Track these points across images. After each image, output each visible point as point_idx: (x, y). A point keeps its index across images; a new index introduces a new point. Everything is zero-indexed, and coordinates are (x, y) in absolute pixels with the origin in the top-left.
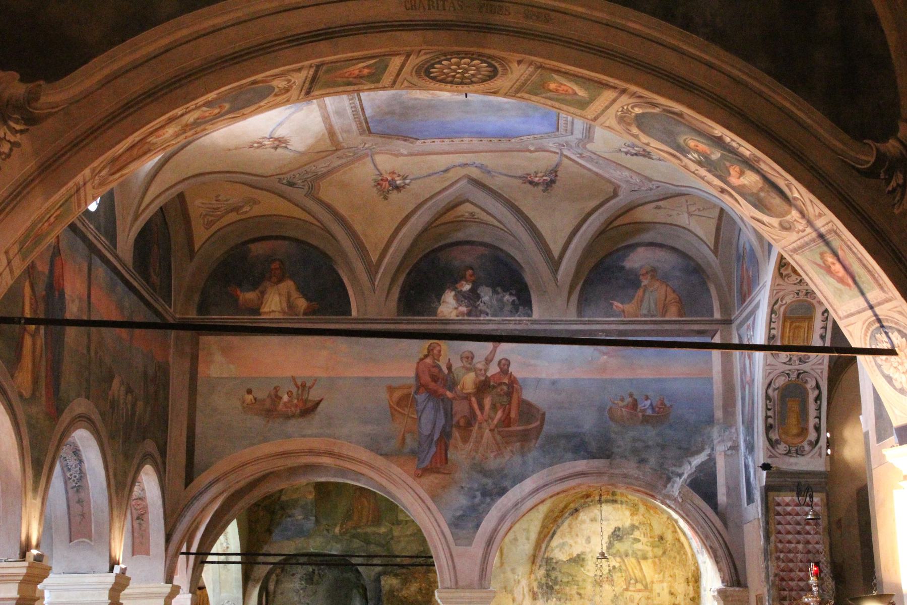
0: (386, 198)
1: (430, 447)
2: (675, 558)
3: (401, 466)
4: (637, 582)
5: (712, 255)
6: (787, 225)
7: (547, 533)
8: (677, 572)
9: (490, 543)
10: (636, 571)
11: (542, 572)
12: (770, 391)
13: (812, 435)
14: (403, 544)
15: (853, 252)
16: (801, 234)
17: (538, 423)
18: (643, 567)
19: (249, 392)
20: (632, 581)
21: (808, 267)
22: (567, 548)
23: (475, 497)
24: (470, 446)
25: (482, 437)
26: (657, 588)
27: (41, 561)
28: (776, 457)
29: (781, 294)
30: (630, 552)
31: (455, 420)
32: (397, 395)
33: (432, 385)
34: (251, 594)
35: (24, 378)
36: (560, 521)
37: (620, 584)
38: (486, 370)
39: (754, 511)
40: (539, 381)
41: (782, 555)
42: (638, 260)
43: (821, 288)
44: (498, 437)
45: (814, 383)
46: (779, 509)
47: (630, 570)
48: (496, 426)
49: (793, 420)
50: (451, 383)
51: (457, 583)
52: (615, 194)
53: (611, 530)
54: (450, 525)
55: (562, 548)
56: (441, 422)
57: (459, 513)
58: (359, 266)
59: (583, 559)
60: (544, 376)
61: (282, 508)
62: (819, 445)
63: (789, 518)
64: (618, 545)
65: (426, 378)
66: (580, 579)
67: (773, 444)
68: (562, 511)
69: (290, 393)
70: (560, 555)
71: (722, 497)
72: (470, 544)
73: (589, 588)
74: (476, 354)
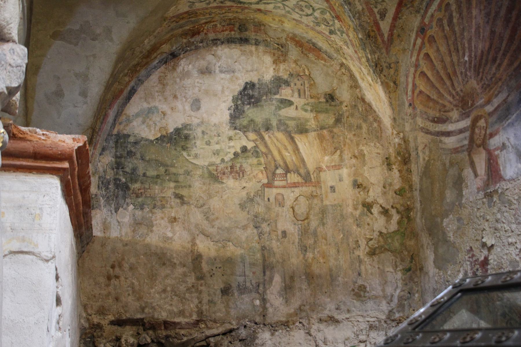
2: (359, 127)
4: (287, 170)
7: (120, 89)
8: (365, 149)
10: (286, 154)
20: (279, 171)
22: (156, 118)
26: (329, 178)
30: (274, 123)
36: (143, 72)
37: (256, 175)
47: (276, 153)
55: (150, 115)
59: (187, 137)
66: (181, 171)
68: (148, 55)
73: (197, 187)
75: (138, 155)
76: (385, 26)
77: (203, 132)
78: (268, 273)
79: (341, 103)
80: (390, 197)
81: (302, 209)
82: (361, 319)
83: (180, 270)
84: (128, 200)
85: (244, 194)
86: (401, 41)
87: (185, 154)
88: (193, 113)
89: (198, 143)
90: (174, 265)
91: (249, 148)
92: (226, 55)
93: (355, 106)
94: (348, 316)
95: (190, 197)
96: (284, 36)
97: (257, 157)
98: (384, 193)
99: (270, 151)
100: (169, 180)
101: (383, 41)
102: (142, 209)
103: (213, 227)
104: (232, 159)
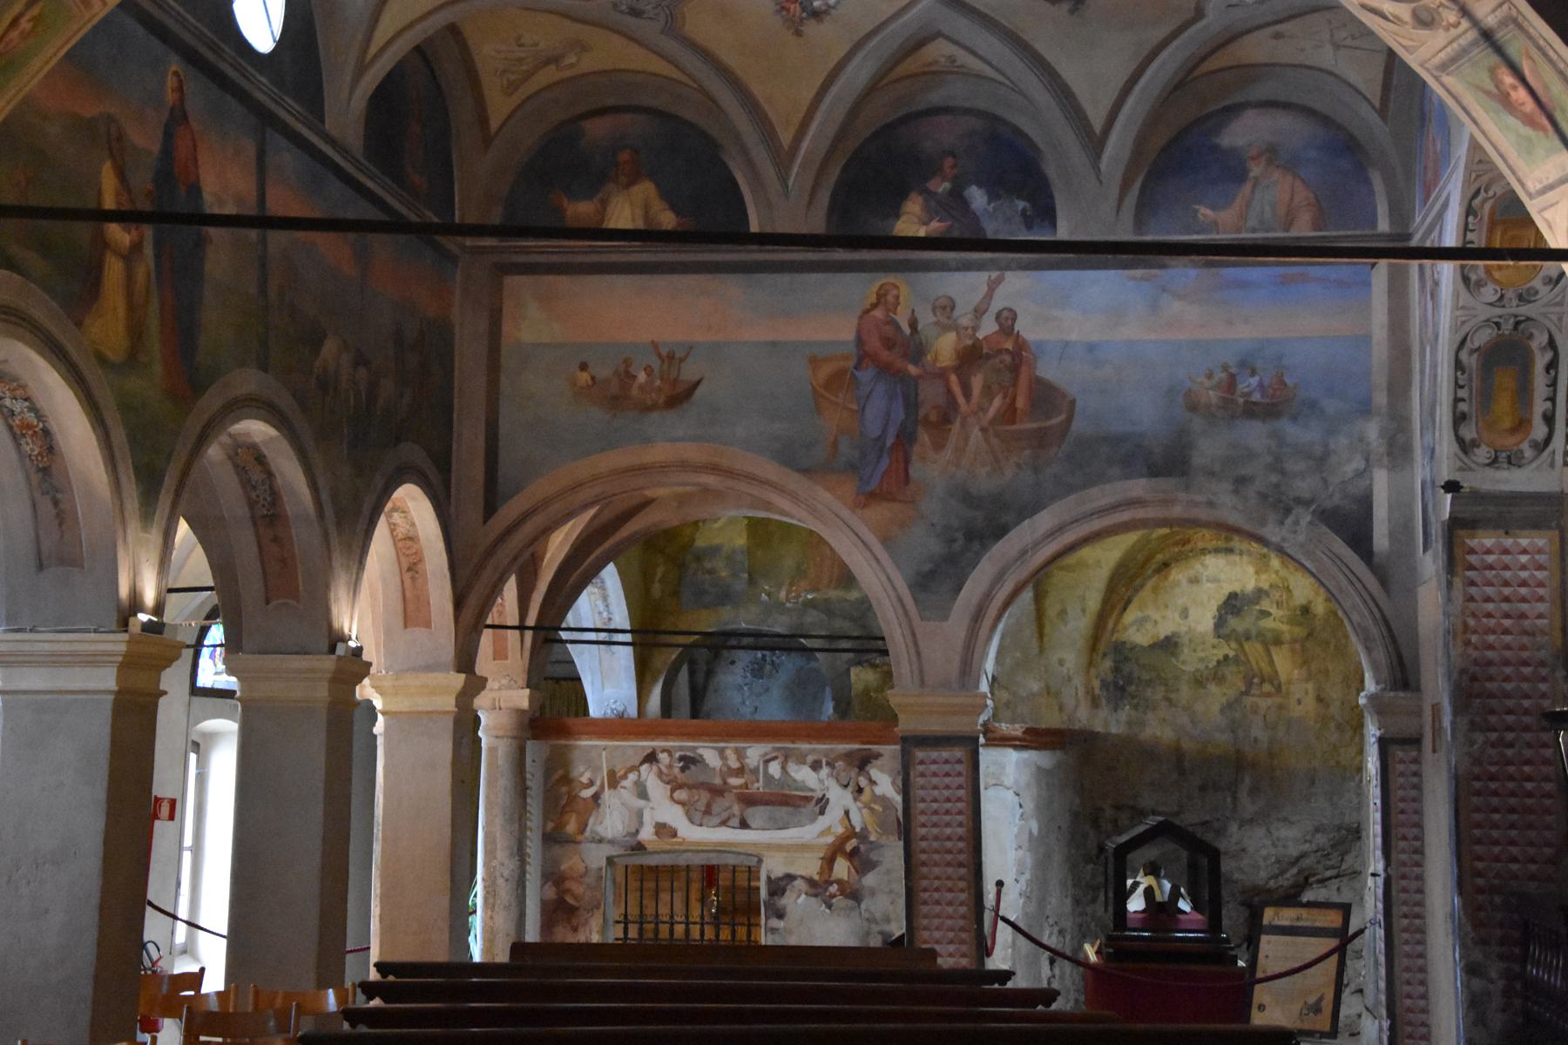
0: (798, 33)
1: (880, 457)
2: (1328, 643)
3: (828, 489)
4: (1263, 681)
5: (1378, 120)
6: (1425, 16)
9: (978, 616)
11: (1108, 664)
12: (1464, 356)
13: (1539, 431)
15: (1550, 61)
16: (1454, 32)
17: (1063, 417)
19: (584, 367)
21: (1469, 99)
22: (1149, 626)
23: (954, 541)
24: (948, 454)
25: (966, 439)
26: (1297, 690)
27: (160, 633)
28: (1471, 469)
29: (1485, 178)
30: (1254, 633)
31: (922, 413)
32: (825, 371)
33: (885, 355)
34: (650, 692)
35: (108, 326)
36: (1138, 582)
37: (1236, 683)
38: (975, 329)
39: (1430, 564)
40: (1067, 344)
41: (1474, 638)
42: (1244, 133)
43: (1493, 138)
44: (995, 441)
45: (1545, 339)
46: (1472, 559)
48: (993, 421)
49: (1503, 405)
50: (916, 349)
51: (922, 683)
52: (1199, 14)
54: (910, 587)
56: (899, 414)
57: (928, 567)
58: (760, 154)
59: (1176, 644)
60: (1074, 337)
61: (698, 559)
62: (1550, 448)
63: (1490, 574)
64: (1234, 623)
65: (874, 343)
67: (1465, 446)
69: (649, 370)
70: (1141, 638)
71: (1381, 540)
72: (946, 618)
73: (1185, 692)
74: (959, 302)
85: (1224, 700)
92: (1214, 565)
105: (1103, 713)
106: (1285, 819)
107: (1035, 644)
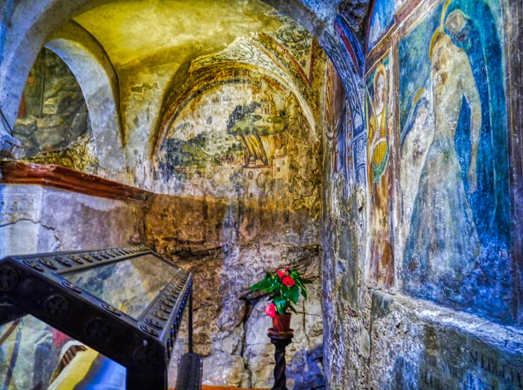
2: (297, 131)
4: (256, 158)
8: (299, 145)
10: (256, 148)
11: (164, 152)
14: (45, 135)
18: (264, 143)
20: (252, 158)
22: (188, 129)
26: (277, 163)
30: (251, 129)
36: (183, 103)
47: (250, 147)
53: (232, 110)
59: (204, 139)
64: (240, 124)
70: (181, 136)
73: (209, 167)
75: (179, 150)
76: (306, 70)
77: (213, 136)
78: (241, 217)
79: (289, 116)
80: (309, 175)
81: (262, 180)
82: (284, 246)
83: (196, 214)
84: (173, 175)
85: (232, 171)
86: (319, 78)
87: (203, 149)
88: (208, 125)
89: (210, 142)
90: (193, 211)
91: (237, 145)
92: (227, 90)
93: (297, 118)
94: (278, 243)
95: (204, 173)
96: (259, 76)
97: (241, 150)
98: (306, 172)
99: (248, 147)
100: (194, 164)
101: (307, 79)
102: (180, 179)
103: (215, 190)
104: (227, 152)
105: (161, 181)
106: (269, 244)
107: (119, 141)
